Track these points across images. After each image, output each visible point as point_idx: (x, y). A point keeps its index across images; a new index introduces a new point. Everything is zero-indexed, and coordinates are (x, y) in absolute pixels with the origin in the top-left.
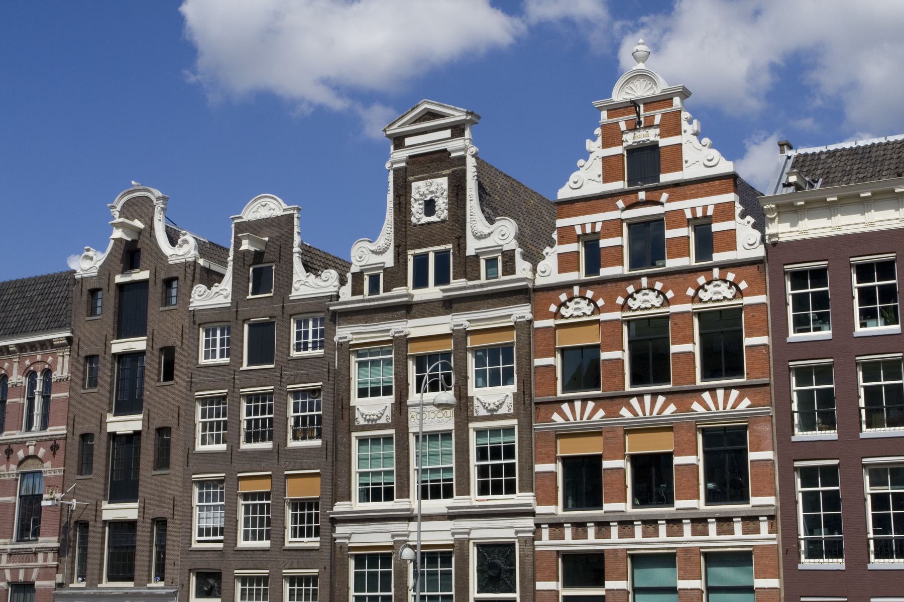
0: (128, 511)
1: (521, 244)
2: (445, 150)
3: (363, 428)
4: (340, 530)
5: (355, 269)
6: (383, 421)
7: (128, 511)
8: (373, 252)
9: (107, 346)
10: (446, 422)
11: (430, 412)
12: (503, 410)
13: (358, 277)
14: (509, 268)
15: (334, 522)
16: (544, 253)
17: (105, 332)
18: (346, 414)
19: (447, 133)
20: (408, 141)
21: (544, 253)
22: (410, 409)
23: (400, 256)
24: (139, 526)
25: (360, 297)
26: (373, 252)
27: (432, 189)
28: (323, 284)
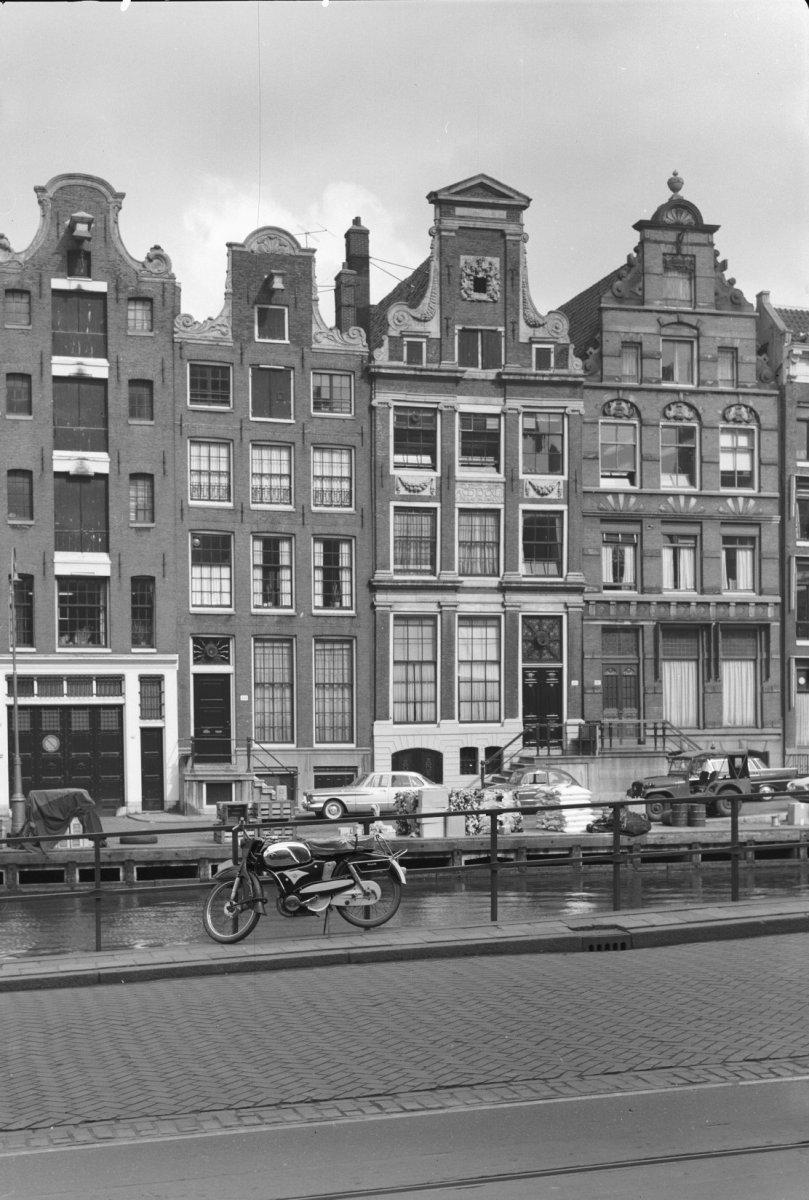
0: (95, 564)
1: (572, 341)
2: (502, 231)
3: (403, 498)
4: (380, 598)
5: (393, 332)
6: (426, 493)
7: (95, 564)
8: (414, 318)
9: (44, 365)
10: (495, 499)
11: (478, 485)
12: (553, 496)
13: (396, 342)
14: (562, 361)
15: (373, 588)
16: (588, 352)
17: (39, 349)
18: (386, 482)
19: (502, 214)
20: (459, 211)
21: (588, 352)
22: (458, 485)
23: (446, 328)
24: (113, 586)
25: (395, 363)
26: (414, 318)
27: (485, 265)
28: (349, 340)
